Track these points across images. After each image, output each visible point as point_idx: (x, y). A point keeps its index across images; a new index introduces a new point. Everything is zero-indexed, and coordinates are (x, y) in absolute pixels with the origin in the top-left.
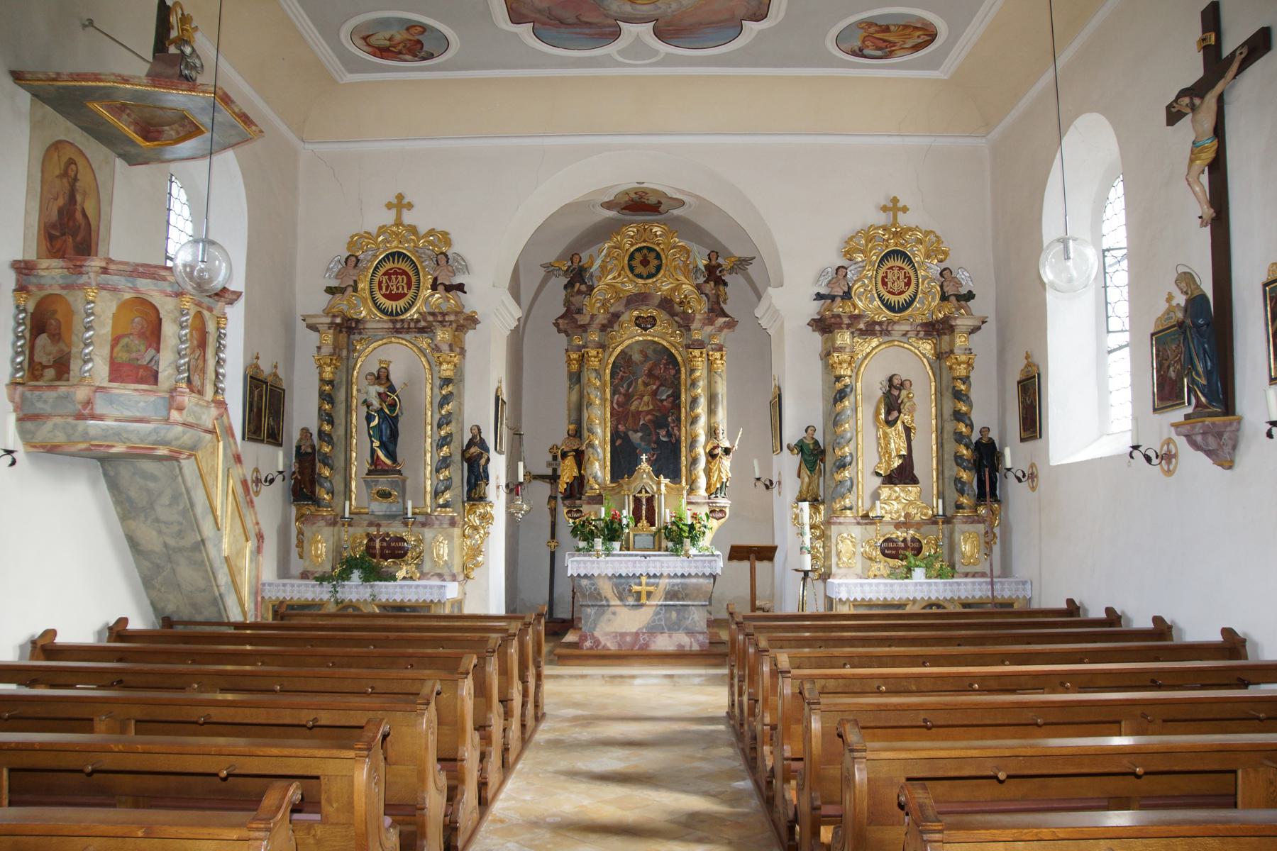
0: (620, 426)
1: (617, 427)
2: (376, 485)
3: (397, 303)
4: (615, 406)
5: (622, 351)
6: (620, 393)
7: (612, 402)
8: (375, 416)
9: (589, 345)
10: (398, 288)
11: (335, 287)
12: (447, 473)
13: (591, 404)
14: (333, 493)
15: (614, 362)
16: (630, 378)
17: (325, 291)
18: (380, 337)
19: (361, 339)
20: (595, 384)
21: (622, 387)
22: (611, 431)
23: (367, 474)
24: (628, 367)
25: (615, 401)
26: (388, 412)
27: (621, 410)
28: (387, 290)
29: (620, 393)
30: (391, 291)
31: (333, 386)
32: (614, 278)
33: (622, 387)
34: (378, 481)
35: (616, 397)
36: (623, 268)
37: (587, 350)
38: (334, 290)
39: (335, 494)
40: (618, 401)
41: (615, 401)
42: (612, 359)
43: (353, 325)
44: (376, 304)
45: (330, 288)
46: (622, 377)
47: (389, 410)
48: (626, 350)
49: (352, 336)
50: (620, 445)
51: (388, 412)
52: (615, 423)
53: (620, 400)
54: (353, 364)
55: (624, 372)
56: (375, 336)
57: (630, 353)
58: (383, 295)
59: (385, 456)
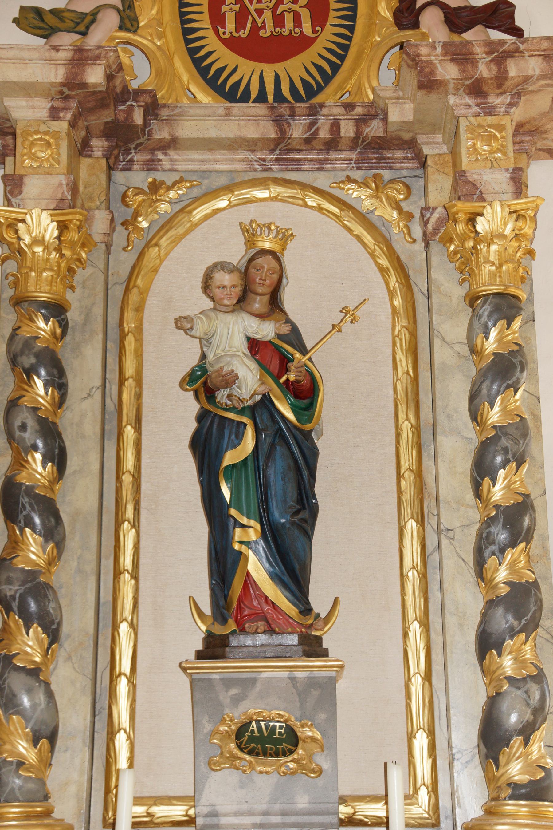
2: (236, 701)
3: (279, 67)
8: (241, 426)
10: (279, 21)
11: (55, 12)
12: (528, 652)
14: (52, 738)
17: (16, 21)
18: (223, 181)
19: (155, 187)
23: (200, 655)
26: (290, 415)
28: (240, 23)
30: (255, 28)
31: (64, 326)
34: (253, 681)
38: (51, 20)
39: (59, 744)
43: (138, 118)
44: (203, 72)
45: (38, 12)
47: (295, 410)
49: (119, 176)
51: (290, 415)
54: (125, 271)
56: (204, 174)
58: (225, 42)
59: (273, 576)
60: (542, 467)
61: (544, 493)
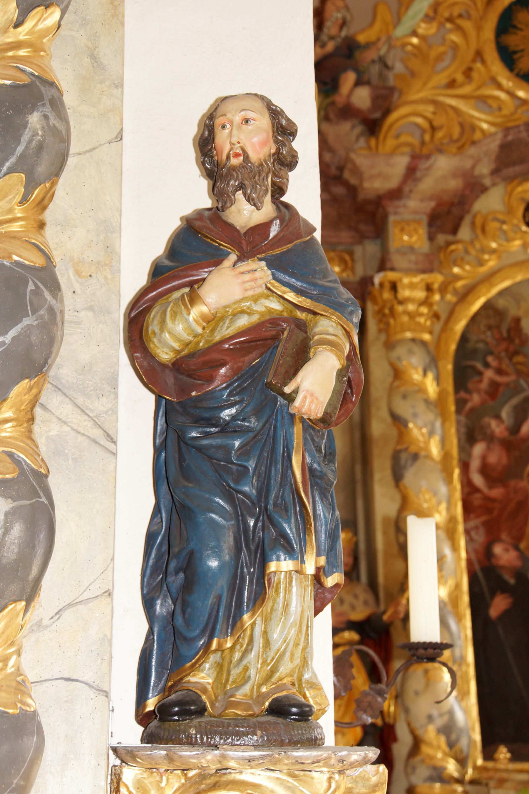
0: (498, 549)
1: (488, 553)
4: (478, 480)
5: (488, 306)
6: (490, 438)
7: (465, 467)
9: (397, 260)
13: (415, 457)
15: (464, 339)
16: (517, 390)
20: (422, 390)
21: (498, 417)
22: (469, 562)
24: (512, 355)
25: (475, 464)
27: (497, 493)
29: (490, 438)
32: (452, 84)
33: (498, 417)
35: (479, 449)
36: (479, 55)
37: (391, 275)
40: (484, 458)
41: (475, 464)
42: (460, 326)
46: (494, 386)
48: (501, 303)
50: (506, 614)
52: (480, 537)
53: (493, 459)
55: (500, 372)
57: (513, 312)
60: (119, 85)
61: (120, 138)
